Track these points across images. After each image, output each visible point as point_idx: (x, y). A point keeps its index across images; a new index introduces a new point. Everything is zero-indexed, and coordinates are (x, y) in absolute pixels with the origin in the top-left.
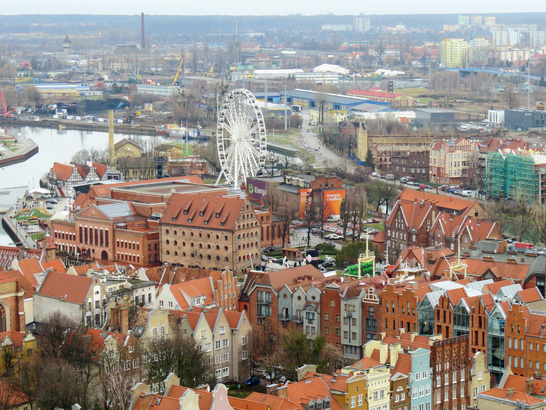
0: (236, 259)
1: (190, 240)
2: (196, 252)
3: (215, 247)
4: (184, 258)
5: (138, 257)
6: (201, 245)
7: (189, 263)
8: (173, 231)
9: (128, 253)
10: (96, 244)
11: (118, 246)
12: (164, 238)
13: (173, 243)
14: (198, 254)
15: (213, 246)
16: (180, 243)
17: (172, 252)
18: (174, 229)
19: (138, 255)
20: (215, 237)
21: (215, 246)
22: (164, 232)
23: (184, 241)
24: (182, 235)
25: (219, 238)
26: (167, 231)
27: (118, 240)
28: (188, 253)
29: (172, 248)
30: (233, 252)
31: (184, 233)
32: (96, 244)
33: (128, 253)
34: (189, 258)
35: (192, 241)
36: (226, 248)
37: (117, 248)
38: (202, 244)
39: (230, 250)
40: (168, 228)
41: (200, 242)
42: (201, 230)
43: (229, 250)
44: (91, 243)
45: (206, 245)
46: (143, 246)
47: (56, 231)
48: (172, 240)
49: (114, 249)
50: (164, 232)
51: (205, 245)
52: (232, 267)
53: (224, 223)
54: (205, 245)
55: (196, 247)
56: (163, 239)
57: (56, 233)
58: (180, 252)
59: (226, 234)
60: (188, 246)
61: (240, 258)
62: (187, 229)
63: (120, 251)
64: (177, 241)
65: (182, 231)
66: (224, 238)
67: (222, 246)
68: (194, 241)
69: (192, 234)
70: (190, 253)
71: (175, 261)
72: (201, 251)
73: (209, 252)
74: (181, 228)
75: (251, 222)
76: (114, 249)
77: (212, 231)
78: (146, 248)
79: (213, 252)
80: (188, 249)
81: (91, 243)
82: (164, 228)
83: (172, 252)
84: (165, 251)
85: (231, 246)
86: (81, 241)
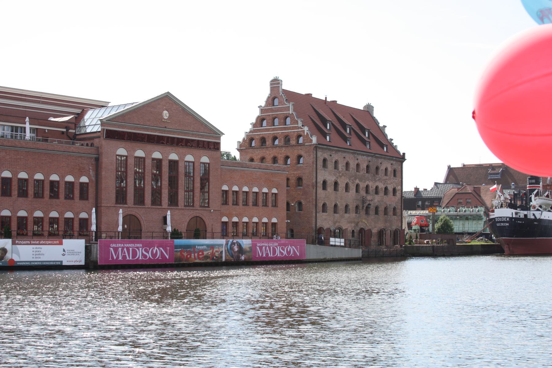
1: (355, 179)
4: (347, 215)
5: (274, 224)
6: (367, 187)
7: (353, 225)
9: (250, 218)
13: (333, 187)
15: (382, 188)
16: (342, 186)
19: (274, 220)
21: (383, 187)
23: (348, 181)
24: (344, 168)
26: (325, 160)
28: (352, 207)
31: (347, 164)
34: (352, 215)
35: (357, 181)
36: (394, 191)
38: (370, 184)
40: (326, 155)
41: (367, 183)
48: (331, 179)
55: (363, 193)
62: (352, 156)
63: (230, 217)
68: (361, 180)
69: (358, 165)
74: (344, 155)
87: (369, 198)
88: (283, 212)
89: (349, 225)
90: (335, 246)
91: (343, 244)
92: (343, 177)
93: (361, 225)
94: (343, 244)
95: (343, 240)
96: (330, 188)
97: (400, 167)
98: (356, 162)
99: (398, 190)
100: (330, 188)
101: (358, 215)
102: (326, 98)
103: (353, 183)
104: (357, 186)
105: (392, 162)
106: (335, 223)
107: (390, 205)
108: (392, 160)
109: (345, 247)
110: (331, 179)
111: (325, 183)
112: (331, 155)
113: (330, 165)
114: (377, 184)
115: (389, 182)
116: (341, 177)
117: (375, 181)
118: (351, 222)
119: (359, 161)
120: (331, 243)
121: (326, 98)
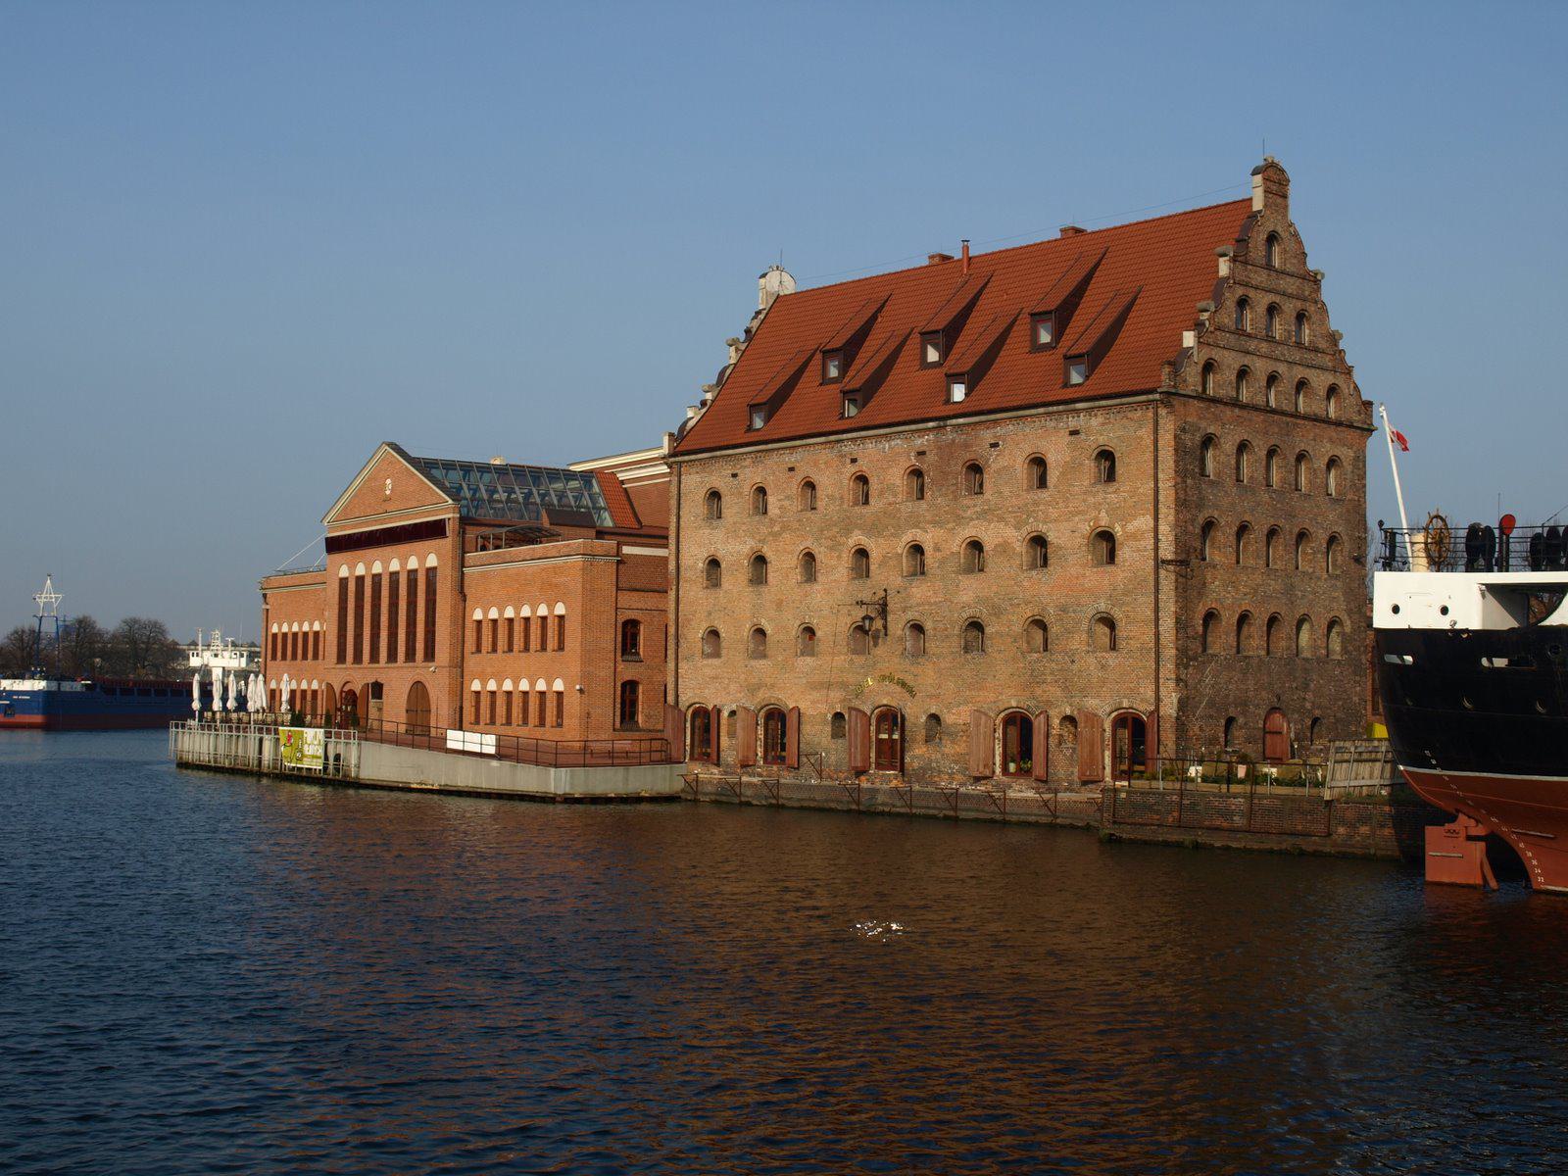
0: (1181, 625)
1: (847, 531)
2: (883, 609)
3: (1020, 547)
6: (917, 549)
7: (836, 695)
8: (747, 490)
10: (392, 656)
11: (479, 650)
12: (696, 544)
14: (897, 624)
15: (1004, 548)
16: (784, 563)
17: (737, 634)
18: (752, 474)
19: (559, 685)
20: (1021, 469)
21: (1016, 538)
22: (694, 506)
23: (808, 543)
24: (796, 505)
25: (1053, 477)
26: (715, 495)
27: (478, 615)
28: (834, 626)
29: (735, 606)
30: (1159, 563)
32: (392, 656)
33: (516, 683)
34: (835, 659)
35: (857, 538)
36: (1106, 542)
37: (471, 662)
38: (927, 539)
39: (1134, 556)
41: (908, 537)
42: (920, 442)
43: (1124, 553)
44: (375, 658)
45: (957, 544)
46: (587, 623)
47: (275, 629)
49: (459, 665)
50: (694, 506)
51: (944, 542)
52: (1150, 694)
53: (1093, 358)
54: (944, 542)
56: (685, 561)
57: (275, 636)
58: (783, 629)
59: (1099, 428)
60: (836, 568)
61: (1210, 617)
62: (825, 455)
64: (768, 553)
65: (799, 476)
66: (1089, 465)
67: (1068, 535)
68: (873, 529)
70: (845, 622)
71: (753, 689)
72: (919, 597)
73: (969, 593)
74: (790, 459)
75: (1299, 373)
76: (459, 665)
77: (988, 436)
78: (608, 639)
79: (1009, 589)
80: (831, 600)
81: (375, 658)
82: (696, 483)
83: (737, 634)
84: (694, 635)
85: (1145, 522)
86: (341, 658)
87: (920, 591)
88: (575, 668)
89: (816, 695)
90: (464, 753)
91: (492, 750)
92: (786, 535)
93: (879, 694)
94: (492, 750)
95: (491, 739)
96: (735, 580)
97: (1145, 433)
98: (851, 469)
99: (1133, 536)
100: (735, 580)
101: (859, 660)
102: (966, 249)
103: (831, 549)
104: (862, 553)
105: (1073, 422)
106: (753, 689)
107: (1064, 609)
108: (1077, 411)
109: (499, 756)
110: (735, 551)
111: (714, 563)
112: (734, 476)
113: (735, 507)
114: (969, 532)
115: (1054, 513)
116: (776, 535)
117: (959, 520)
118: (829, 686)
119: (863, 466)
120: (450, 745)
121: (966, 249)
